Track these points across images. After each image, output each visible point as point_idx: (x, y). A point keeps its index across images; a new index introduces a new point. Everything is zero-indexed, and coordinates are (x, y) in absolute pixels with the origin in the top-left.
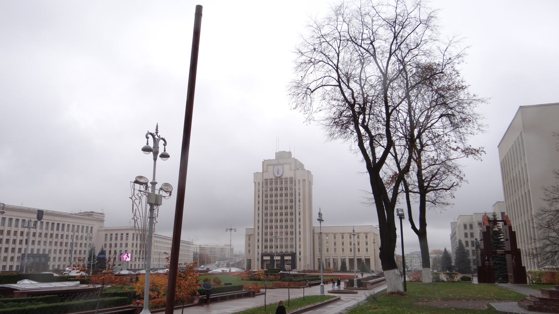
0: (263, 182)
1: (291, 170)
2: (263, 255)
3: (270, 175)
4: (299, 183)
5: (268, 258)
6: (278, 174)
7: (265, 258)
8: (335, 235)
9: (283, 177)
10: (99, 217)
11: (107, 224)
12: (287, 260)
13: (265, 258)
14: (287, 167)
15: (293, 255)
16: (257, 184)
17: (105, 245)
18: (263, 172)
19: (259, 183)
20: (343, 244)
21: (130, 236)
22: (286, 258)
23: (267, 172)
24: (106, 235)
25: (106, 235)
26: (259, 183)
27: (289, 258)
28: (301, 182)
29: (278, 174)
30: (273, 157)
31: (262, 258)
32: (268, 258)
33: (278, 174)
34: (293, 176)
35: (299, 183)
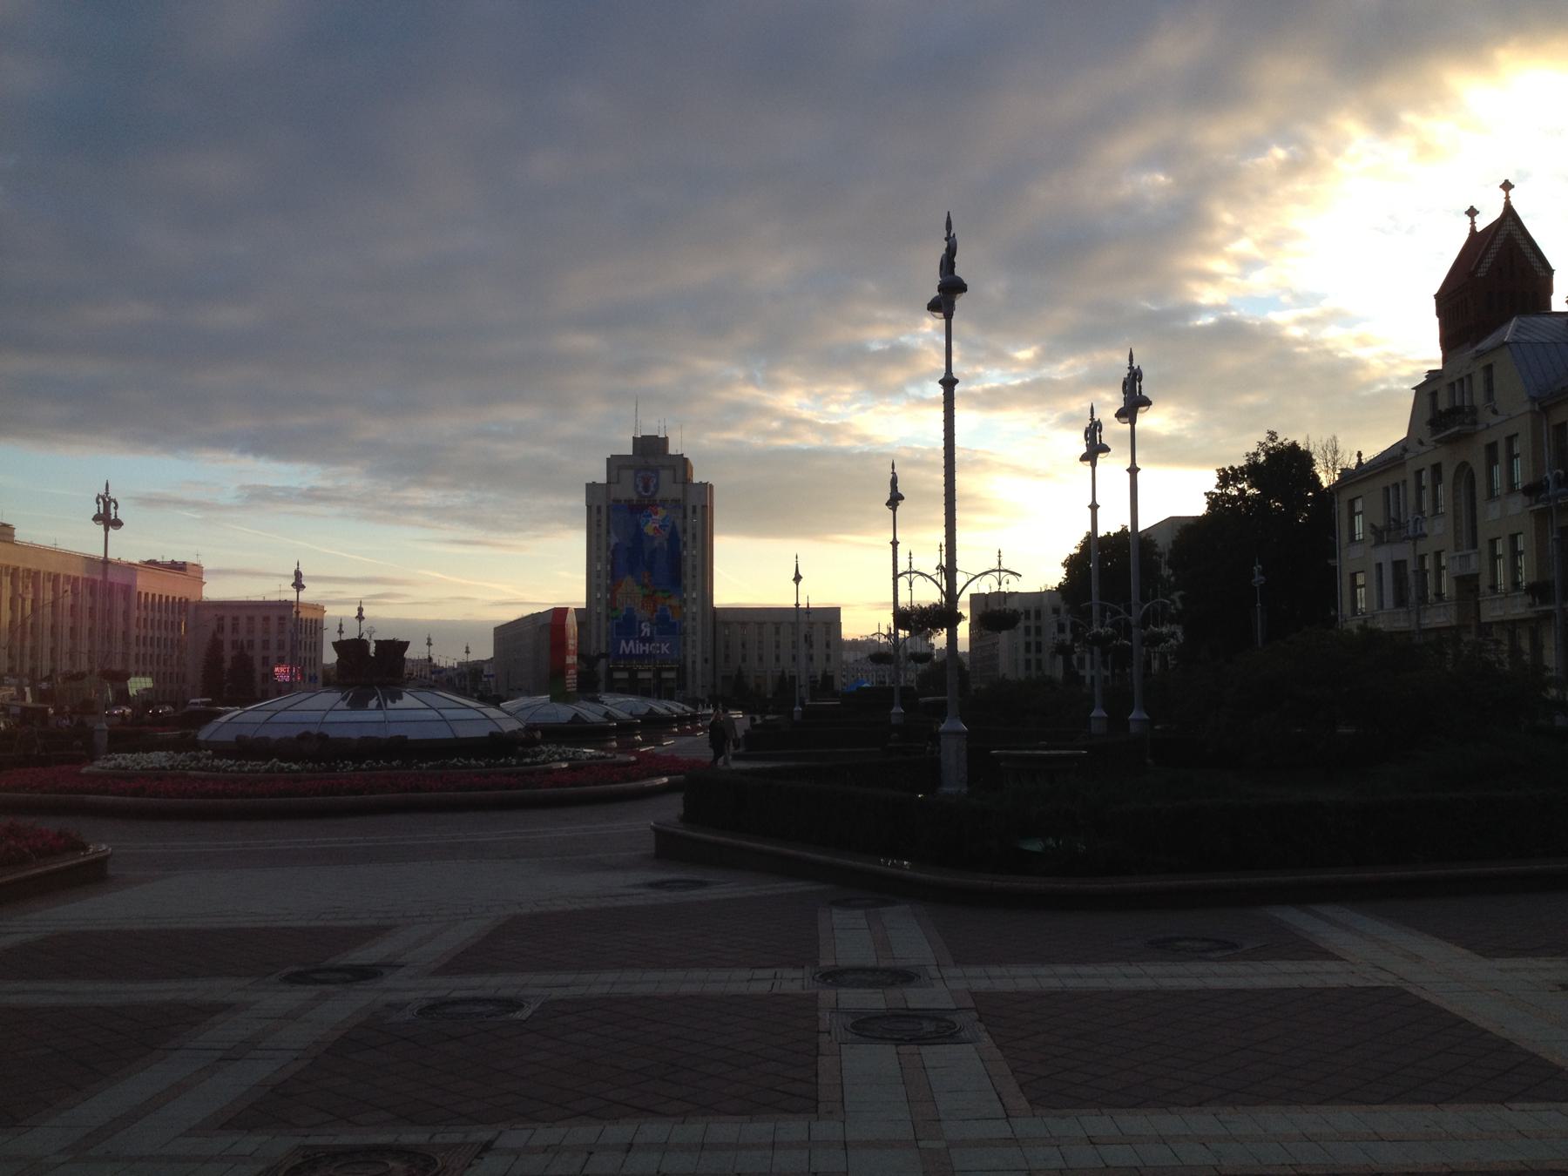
0: (608, 507)
1: (675, 482)
3: (627, 491)
4: (694, 511)
5: (625, 675)
6: (646, 492)
7: (617, 675)
8: (761, 624)
12: (667, 679)
14: (665, 475)
16: (594, 509)
18: (608, 482)
19: (599, 509)
20: (778, 647)
22: (665, 675)
23: (618, 482)
26: (599, 509)
27: (672, 675)
28: (699, 510)
29: (646, 488)
30: (630, 452)
32: (625, 675)
33: (646, 488)
34: (680, 496)
35: (694, 511)
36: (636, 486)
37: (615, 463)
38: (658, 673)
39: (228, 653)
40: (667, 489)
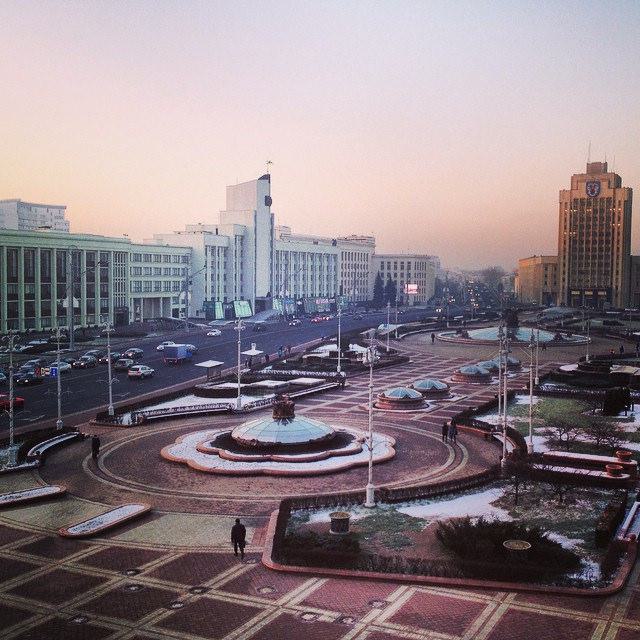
2: (570, 290)
3: (582, 194)
4: (620, 205)
7: (573, 293)
9: (600, 196)
10: (370, 242)
11: (379, 251)
12: (600, 296)
13: (573, 293)
14: (604, 185)
15: (609, 290)
17: (382, 274)
21: (413, 266)
22: (600, 293)
24: (382, 263)
25: (382, 263)
29: (593, 192)
31: (569, 293)
33: (593, 192)
35: (620, 205)
36: (587, 192)
37: (575, 179)
38: (595, 292)
39: (385, 279)
40: (606, 192)
